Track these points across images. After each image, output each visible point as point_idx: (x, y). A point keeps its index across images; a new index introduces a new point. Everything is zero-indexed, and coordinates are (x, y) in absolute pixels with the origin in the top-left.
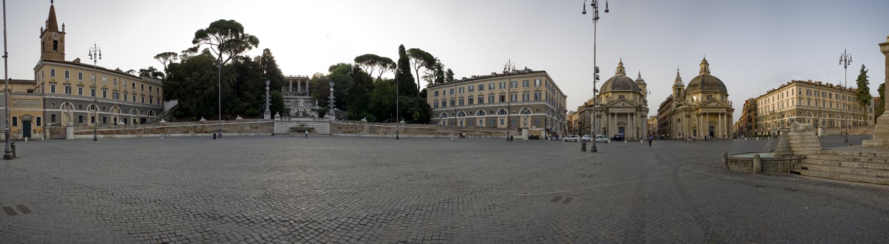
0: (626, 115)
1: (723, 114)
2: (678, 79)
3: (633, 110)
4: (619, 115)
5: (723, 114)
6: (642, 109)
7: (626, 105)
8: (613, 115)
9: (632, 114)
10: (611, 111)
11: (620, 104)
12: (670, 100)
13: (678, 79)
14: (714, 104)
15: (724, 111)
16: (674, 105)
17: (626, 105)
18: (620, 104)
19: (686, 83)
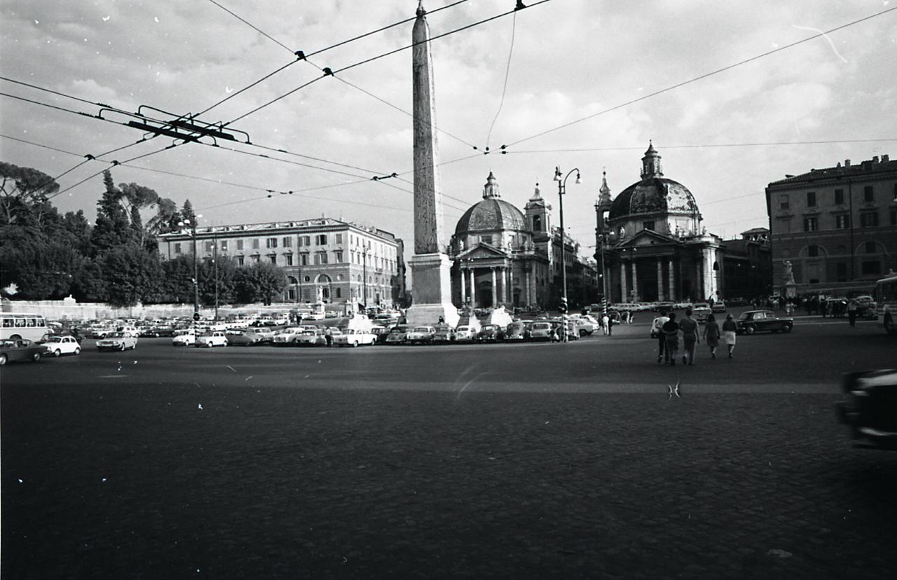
0: (489, 271)
2: (605, 192)
13: (605, 192)
19: (614, 195)
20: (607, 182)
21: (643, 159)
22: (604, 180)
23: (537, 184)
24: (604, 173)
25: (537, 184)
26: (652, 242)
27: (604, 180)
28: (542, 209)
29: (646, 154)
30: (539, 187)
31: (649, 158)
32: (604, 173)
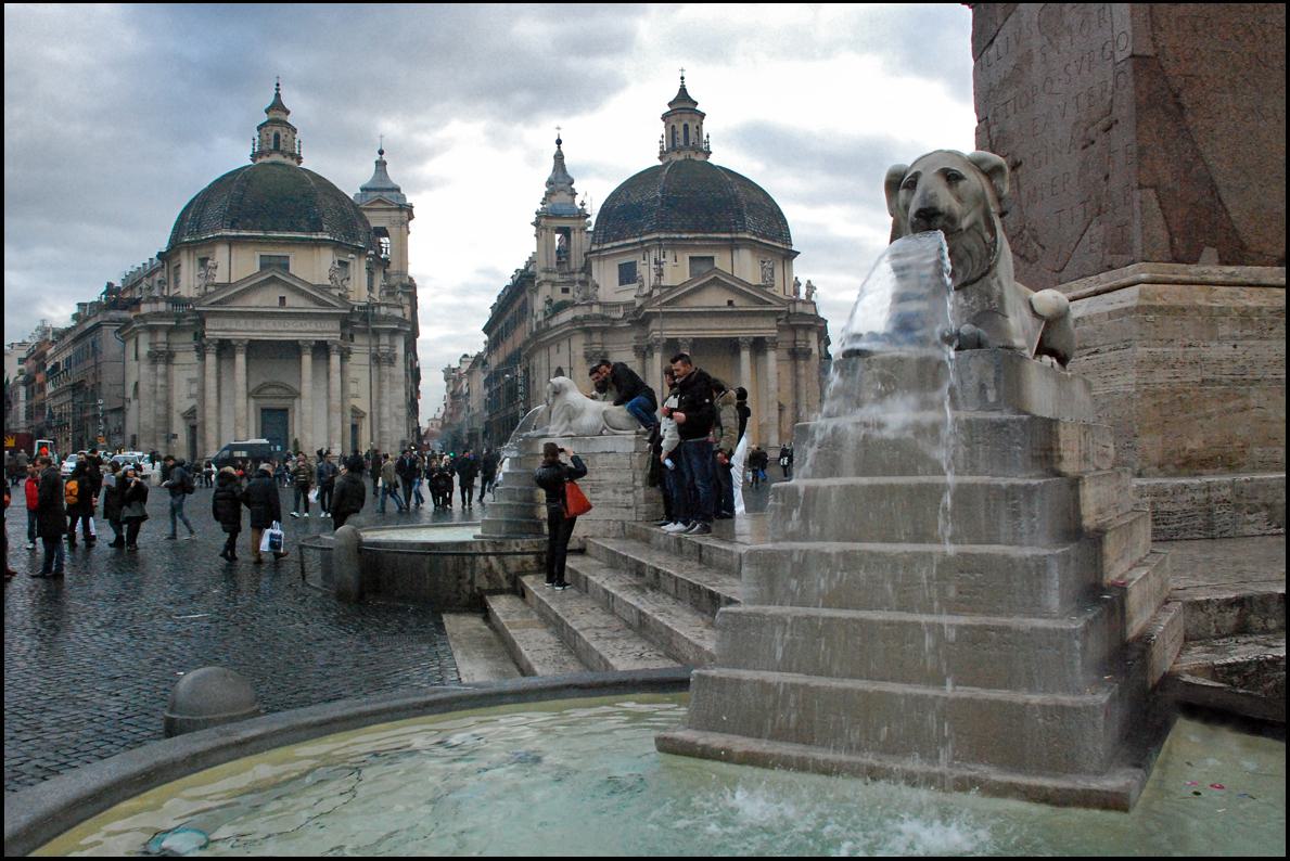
0: (292, 350)
1: (759, 346)
2: (561, 180)
3: (330, 331)
4: (255, 349)
5: (759, 346)
6: (388, 321)
7: (295, 302)
8: (225, 348)
9: (322, 350)
10: (215, 330)
11: (266, 299)
12: (523, 282)
13: (561, 180)
14: (715, 299)
15: (766, 328)
16: (539, 304)
17: (295, 302)
18: (266, 299)
19: (592, 195)
20: (566, 161)
21: (665, 117)
22: (559, 157)
23: (381, 152)
24: (559, 142)
25: (381, 152)
26: (730, 303)
27: (559, 157)
28: (395, 214)
29: (670, 104)
30: (384, 157)
31: (683, 112)
32: (559, 142)
